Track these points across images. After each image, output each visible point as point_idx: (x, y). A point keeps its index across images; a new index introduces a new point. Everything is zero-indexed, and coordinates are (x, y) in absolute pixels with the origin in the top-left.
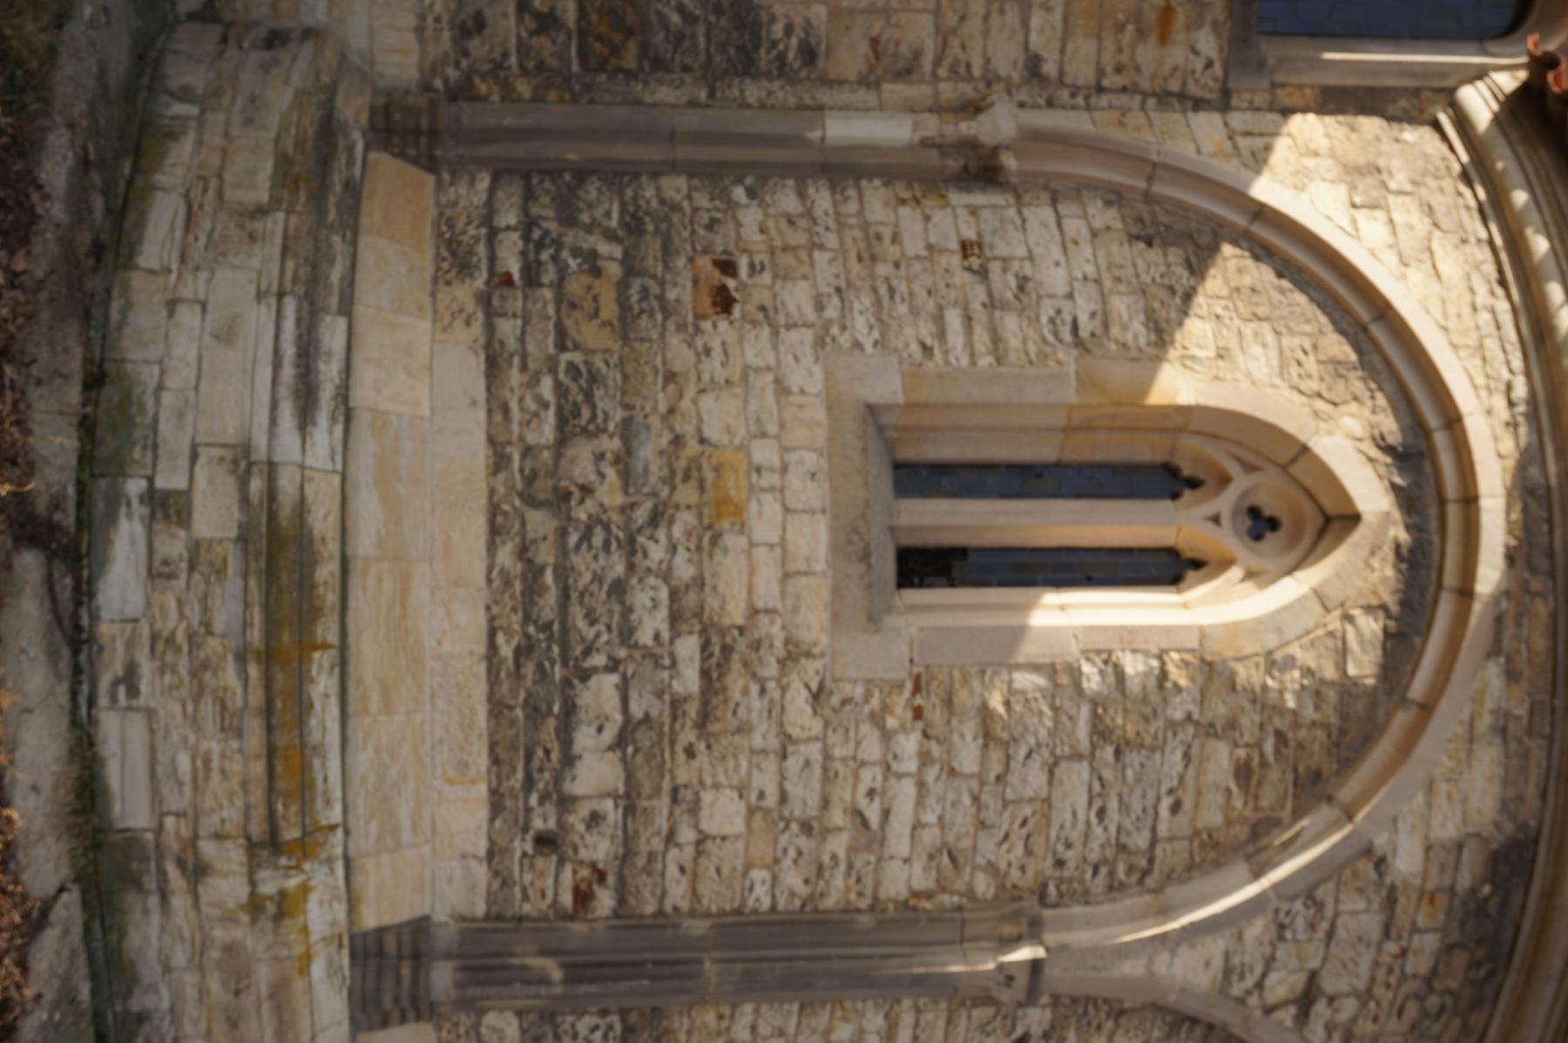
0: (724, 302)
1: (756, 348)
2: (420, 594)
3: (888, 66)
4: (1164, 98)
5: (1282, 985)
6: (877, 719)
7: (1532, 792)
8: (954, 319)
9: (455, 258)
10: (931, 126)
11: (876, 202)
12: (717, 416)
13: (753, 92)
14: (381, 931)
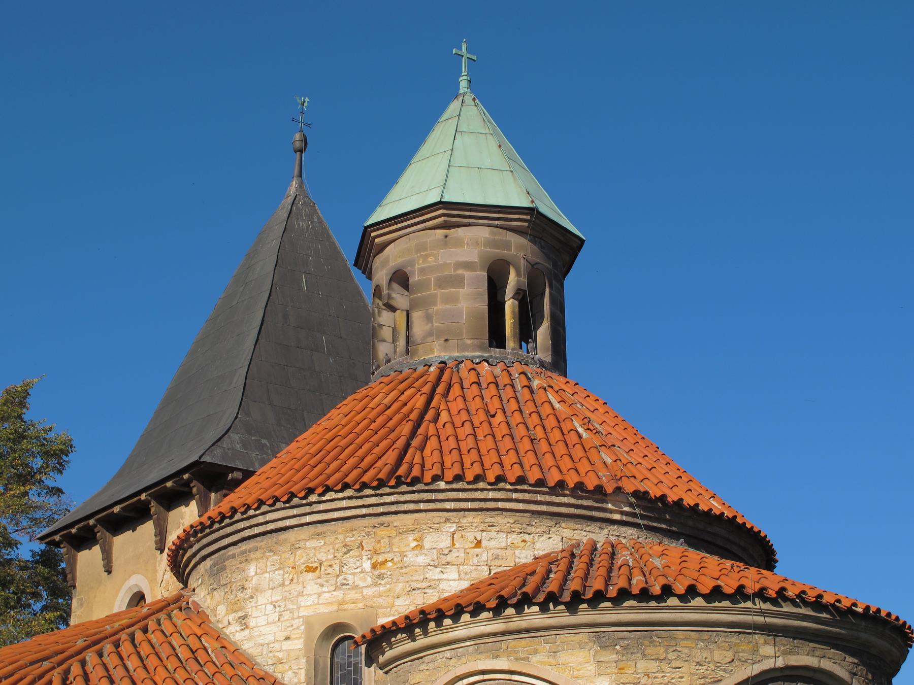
7: (577, 637)
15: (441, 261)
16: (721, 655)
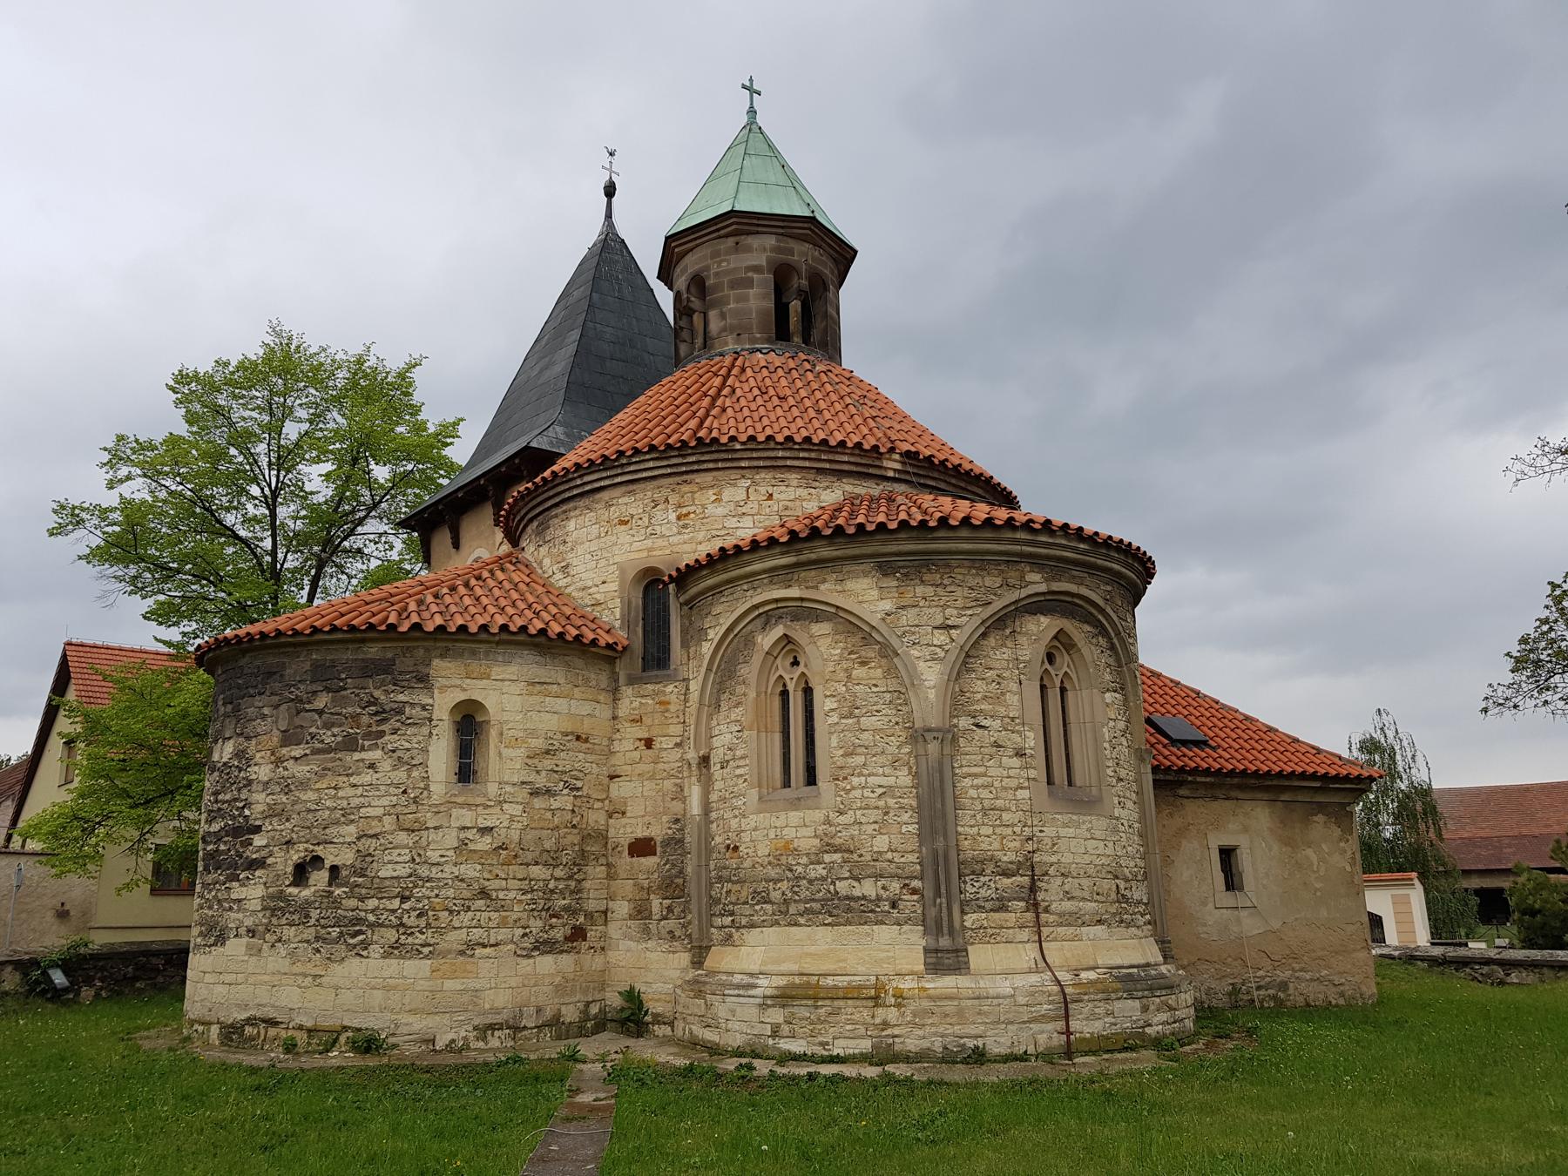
0: (736, 848)
1: (746, 837)
2: (812, 949)
3: (680, 795)
4: (686, 701)
5: (940, 638)
6: (848, 792)
7: (861, 567)
8: (738, 772)
9: (728, 940)
11: (714, 797)
12: (763, 850)
14: (925, 964)
15: (732, 266)
16: (992, 581)
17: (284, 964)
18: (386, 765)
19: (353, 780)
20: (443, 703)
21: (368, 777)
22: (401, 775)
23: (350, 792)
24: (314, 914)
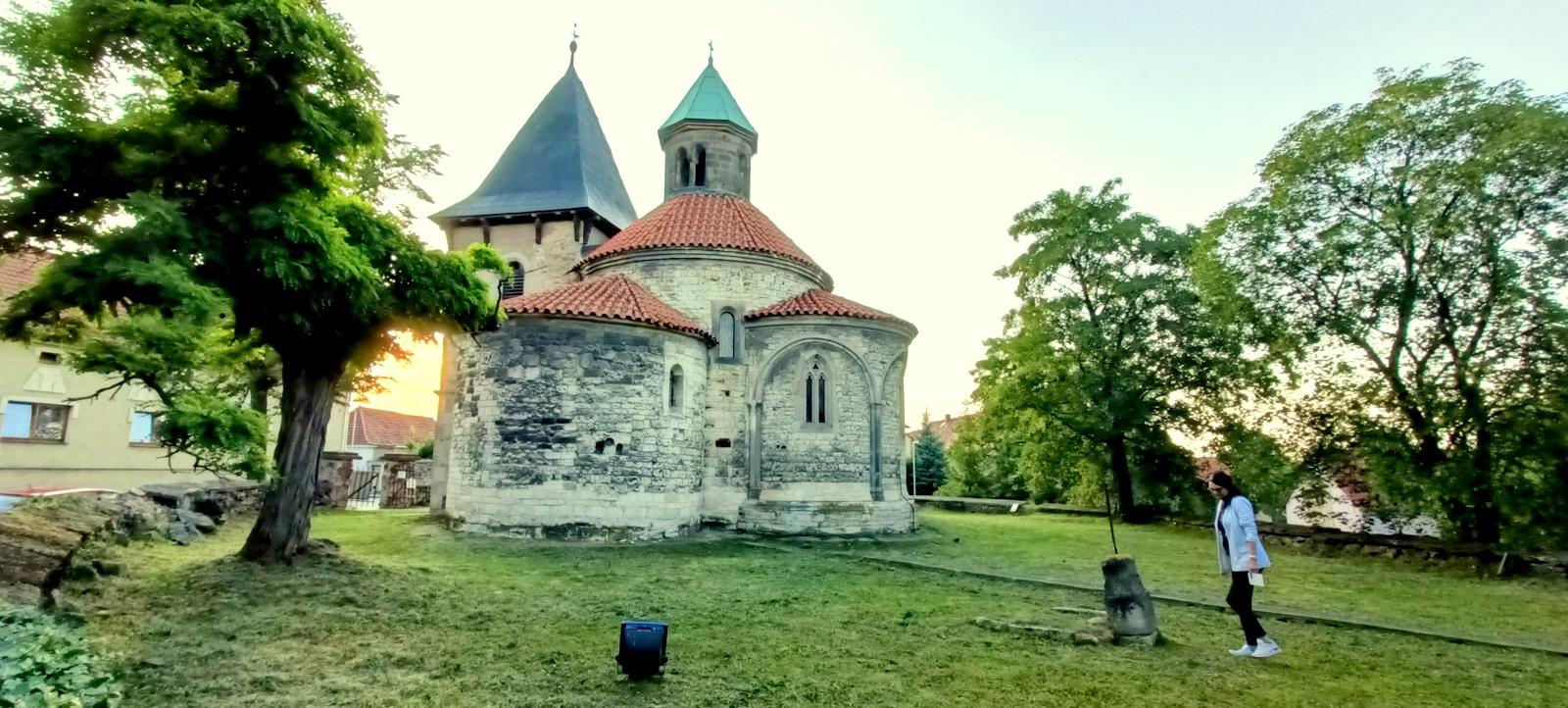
9: (777, 487)
10: (753, 413)
12: (802, 449)
13: (747, 441)
17: (594, 495)
18: (645, 393)
19: (630, 400)
20: (668, 365)
21: (637, 399)
22: (651, 400)
23: (628, 406)
24: (610, 469)
